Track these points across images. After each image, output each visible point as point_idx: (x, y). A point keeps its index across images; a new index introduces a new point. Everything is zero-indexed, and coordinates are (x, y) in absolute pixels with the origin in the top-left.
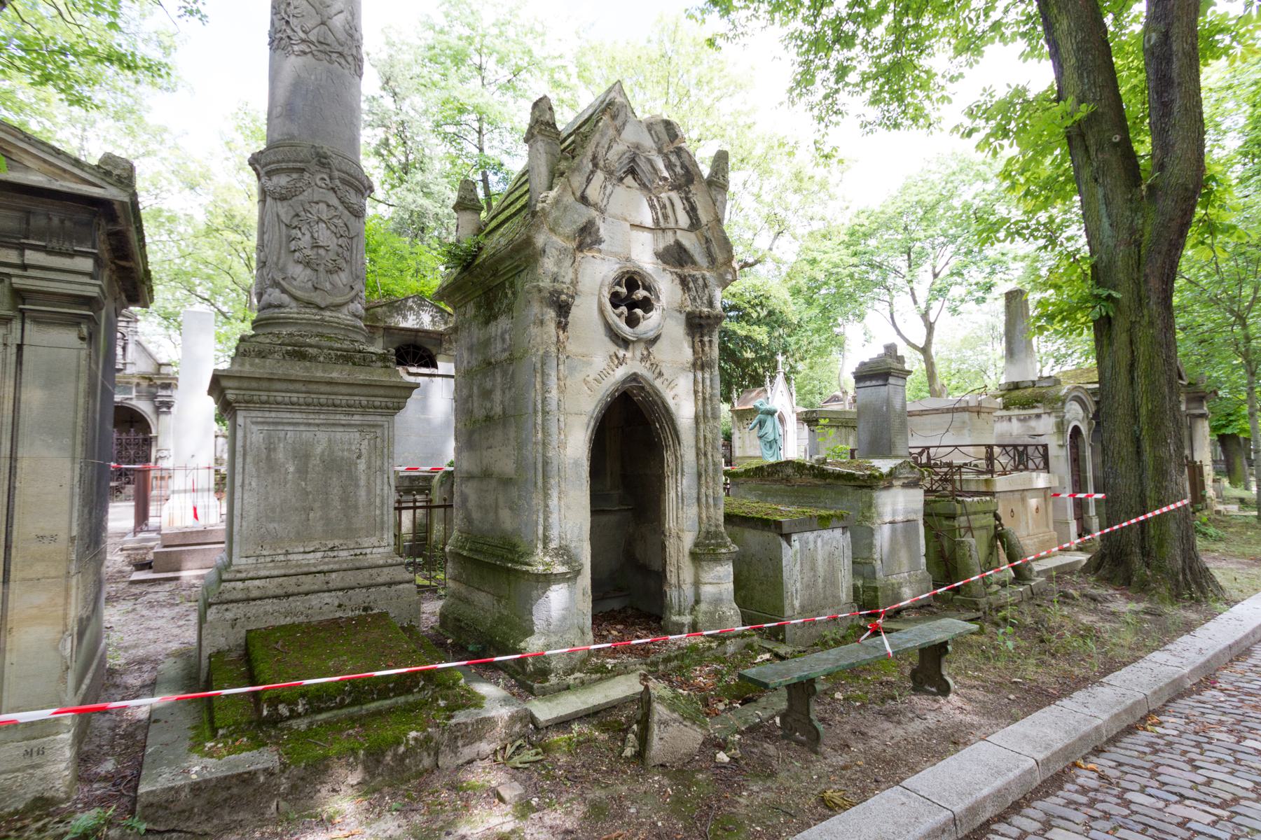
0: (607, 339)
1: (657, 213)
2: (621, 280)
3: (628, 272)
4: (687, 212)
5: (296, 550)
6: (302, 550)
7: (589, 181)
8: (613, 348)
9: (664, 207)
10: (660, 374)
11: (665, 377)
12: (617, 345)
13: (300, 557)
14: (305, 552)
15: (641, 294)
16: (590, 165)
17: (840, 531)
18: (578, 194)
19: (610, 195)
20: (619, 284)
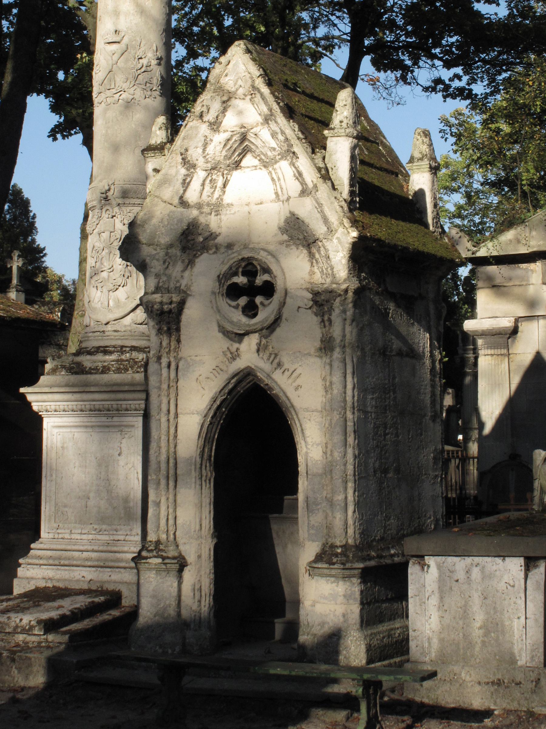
0: (220, 335)
1: (276, 186)
2: (237, 269)
3: (243, 259)
4: (297, 178)
5: (76, 531)
6: (80, 531)
7: (186, 184)
8: (223, 343)
9: (279, 179)
10: (279, 365)
11: (286, 366)
12: (231, 339)
13: (79, 537)
14: (81, 534)
15: (260, 280)
16: (183, 171)
17: (521, 561)
18: (176, 201)
19: (225, 186)
20: (235, 274)
